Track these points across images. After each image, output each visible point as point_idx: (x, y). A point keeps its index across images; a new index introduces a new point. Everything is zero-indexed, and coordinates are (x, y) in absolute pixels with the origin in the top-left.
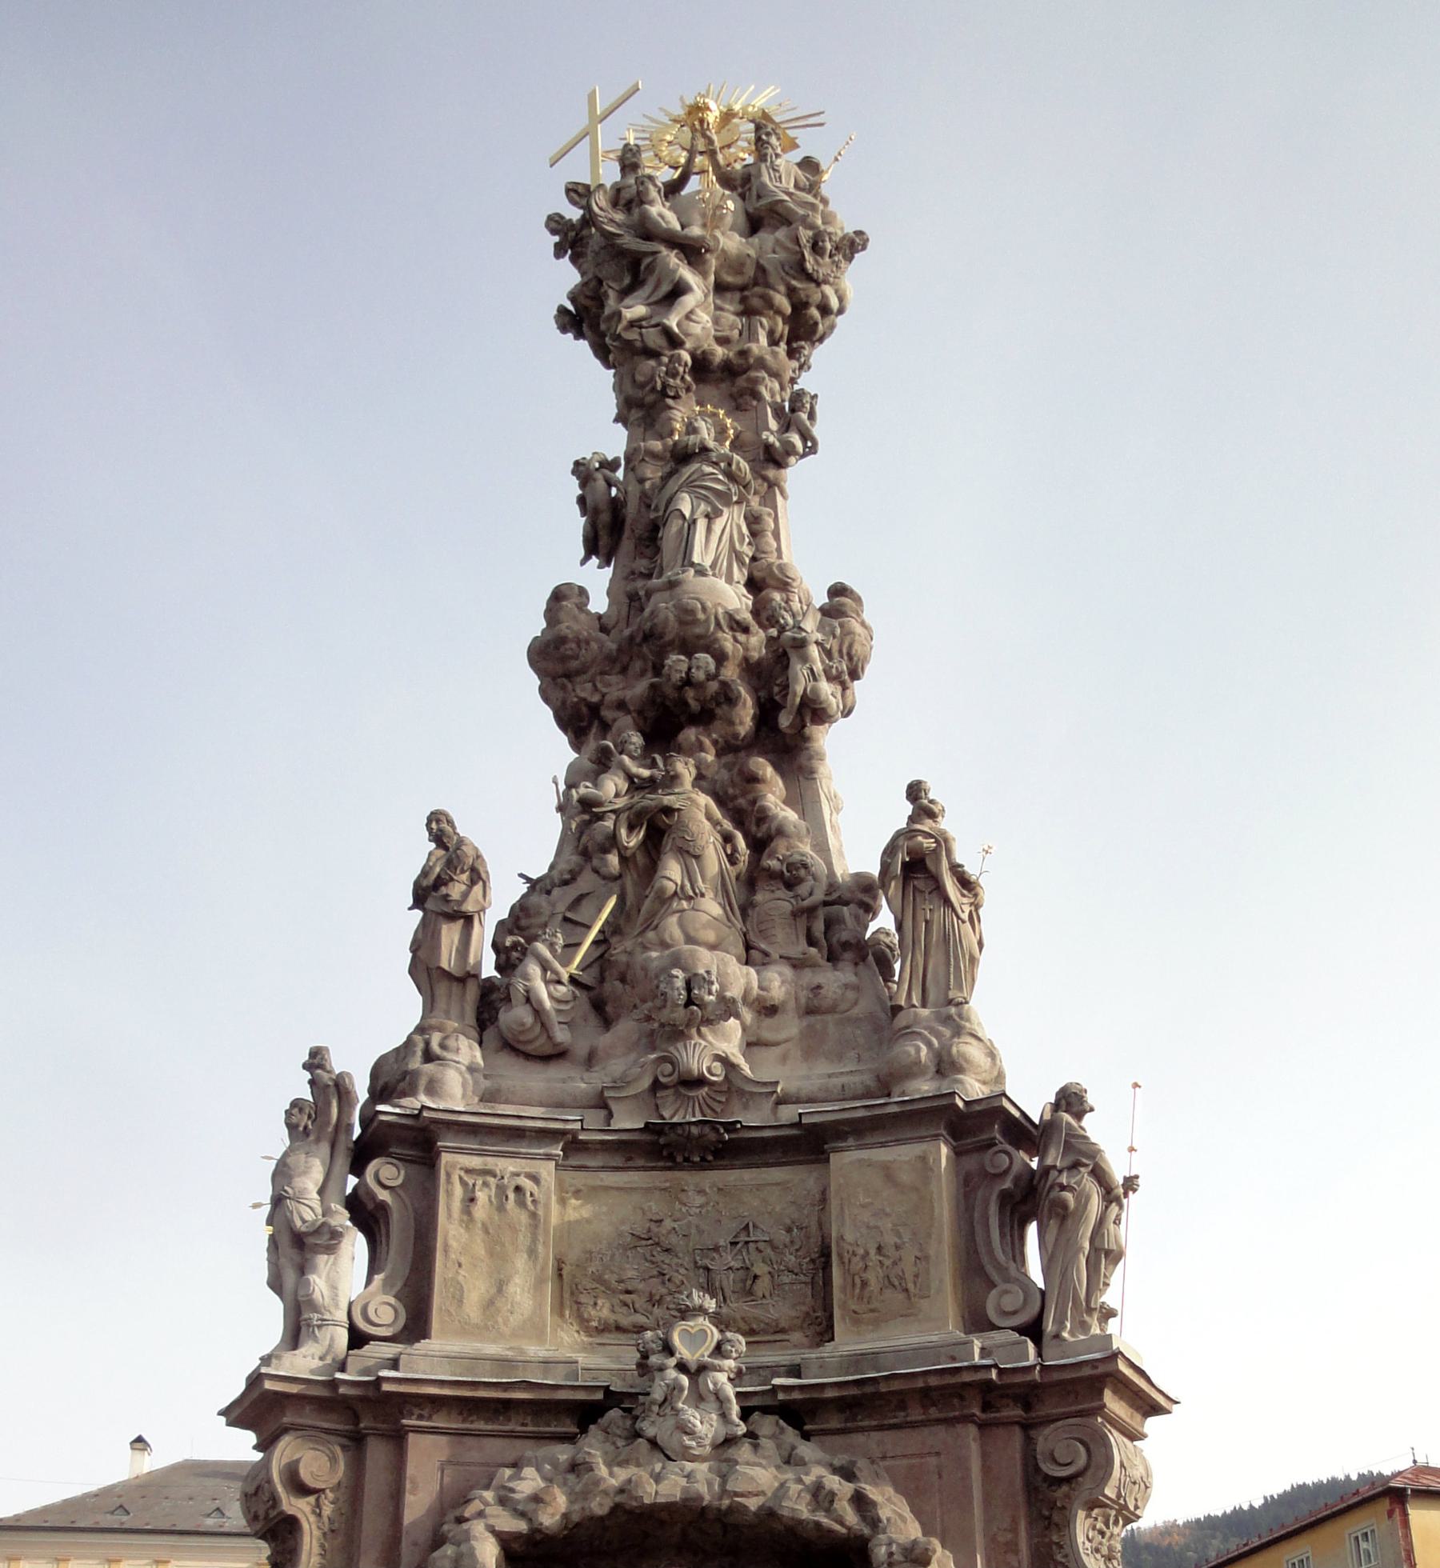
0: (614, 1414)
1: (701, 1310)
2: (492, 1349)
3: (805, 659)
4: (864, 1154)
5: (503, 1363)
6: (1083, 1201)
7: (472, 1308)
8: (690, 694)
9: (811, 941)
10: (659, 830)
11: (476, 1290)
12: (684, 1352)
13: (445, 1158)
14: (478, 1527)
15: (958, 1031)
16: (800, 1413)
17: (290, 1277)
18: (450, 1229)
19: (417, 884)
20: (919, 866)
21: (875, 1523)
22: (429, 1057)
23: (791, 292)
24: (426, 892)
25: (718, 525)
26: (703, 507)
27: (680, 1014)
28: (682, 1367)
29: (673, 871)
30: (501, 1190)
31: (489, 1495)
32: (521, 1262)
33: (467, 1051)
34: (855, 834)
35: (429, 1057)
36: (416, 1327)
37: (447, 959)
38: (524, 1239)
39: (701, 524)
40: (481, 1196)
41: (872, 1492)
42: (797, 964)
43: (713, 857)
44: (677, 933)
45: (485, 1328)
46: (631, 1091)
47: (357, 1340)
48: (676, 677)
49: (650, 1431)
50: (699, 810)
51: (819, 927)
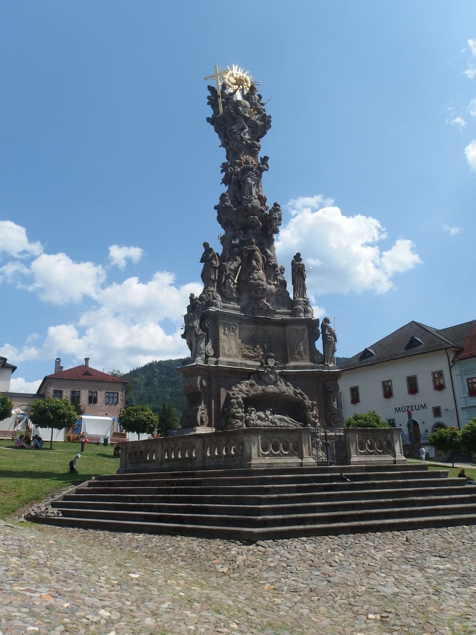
4: (293, 327)
8: (252, 224)
13: (220, 320)
16: (286, 377)
36: (216, 355)
46: (249, 309)
48: (251, 221)
49: (264, 379)
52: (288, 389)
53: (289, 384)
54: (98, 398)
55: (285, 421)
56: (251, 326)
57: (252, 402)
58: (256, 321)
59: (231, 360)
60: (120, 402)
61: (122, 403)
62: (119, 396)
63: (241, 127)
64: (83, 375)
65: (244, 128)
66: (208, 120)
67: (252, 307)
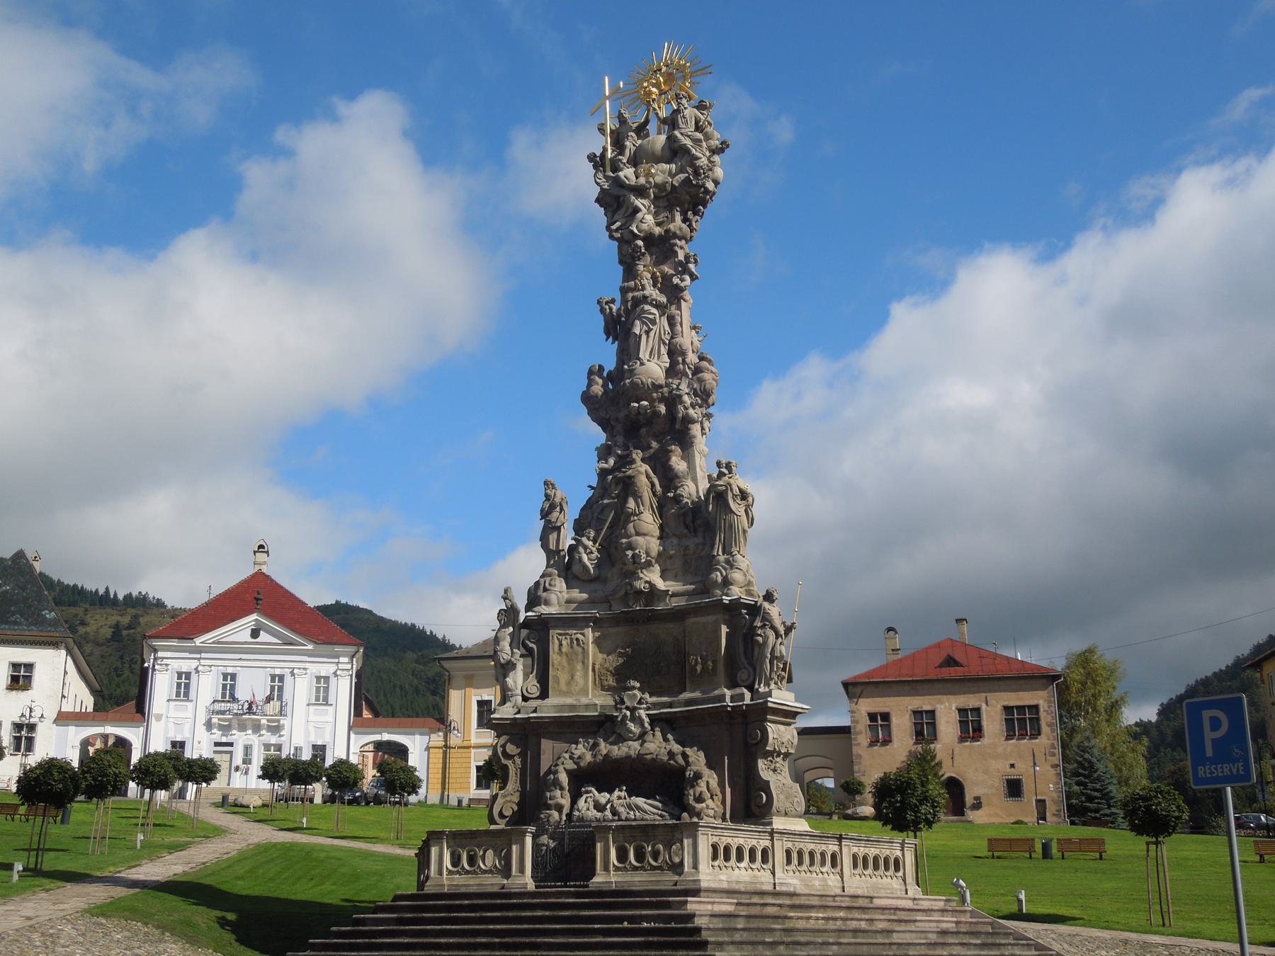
0: (608, 724)
1: (634, 688)
2: (569, 701)
3: (682, 402)
5: (572, 707)
6: (766, 638)
7: (563, 687)
8: (641, 417)
9: (687, 527)
10: (628, 487)
11: (563, 678)
12: (628, 703)
14: (561, 768)
15: (732, 567)
17: (501, 679)
18: (554, 657)
19: (542, 510)
20: (718, 496)
21: (688, 763)
22: (545, 590)
23: (688, 193)
24: (545, 514)
25: (652, 334)
26: (645, 328)
27: (631, 567)
28: (627, 708)
29: (631, 504)
30: (572, 641)
31: (567, 756)
32: (579, 666)
33: (560, 584)
34: (694, 489)
35: (545, 590)
36: (544, 694)
37: (552, 546)
38: (580, 657)
39: (644, 337)
40: (564, 642)
41: (688, 751)
42: (679, 537)
43: (646, 494)
44: (632, 531)
45: (568, 693)
47: (525, 699)
50: (641, 471)
51: (689, 519)
52: (658, 746)
53: (670, 736)
54: (984, 723)
55: (638, 808)
56: (620, 629)
57: (581, 779)
58: (629, 619)
59: (569, 701)
60: (1045, 728)
61: (1053, 731)
62: (1042, 714)
63: (631, 210)
64: (941, 666)
65: (636, 210)
66: (597, 201)
67: (623, 592)
